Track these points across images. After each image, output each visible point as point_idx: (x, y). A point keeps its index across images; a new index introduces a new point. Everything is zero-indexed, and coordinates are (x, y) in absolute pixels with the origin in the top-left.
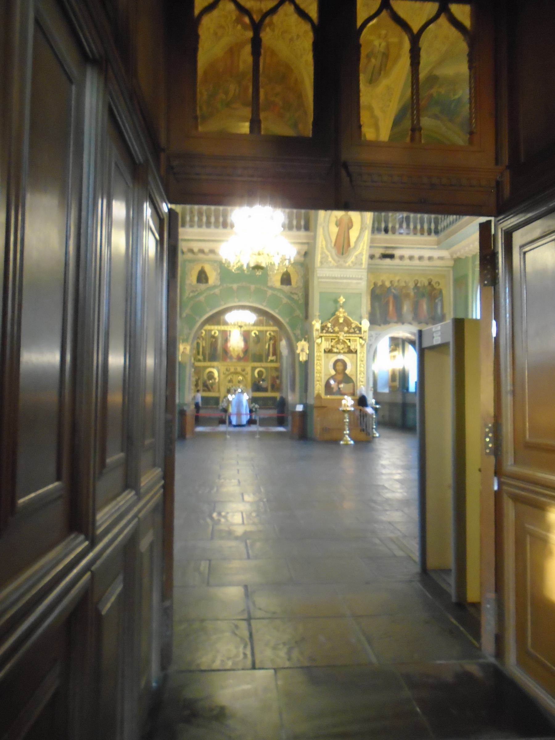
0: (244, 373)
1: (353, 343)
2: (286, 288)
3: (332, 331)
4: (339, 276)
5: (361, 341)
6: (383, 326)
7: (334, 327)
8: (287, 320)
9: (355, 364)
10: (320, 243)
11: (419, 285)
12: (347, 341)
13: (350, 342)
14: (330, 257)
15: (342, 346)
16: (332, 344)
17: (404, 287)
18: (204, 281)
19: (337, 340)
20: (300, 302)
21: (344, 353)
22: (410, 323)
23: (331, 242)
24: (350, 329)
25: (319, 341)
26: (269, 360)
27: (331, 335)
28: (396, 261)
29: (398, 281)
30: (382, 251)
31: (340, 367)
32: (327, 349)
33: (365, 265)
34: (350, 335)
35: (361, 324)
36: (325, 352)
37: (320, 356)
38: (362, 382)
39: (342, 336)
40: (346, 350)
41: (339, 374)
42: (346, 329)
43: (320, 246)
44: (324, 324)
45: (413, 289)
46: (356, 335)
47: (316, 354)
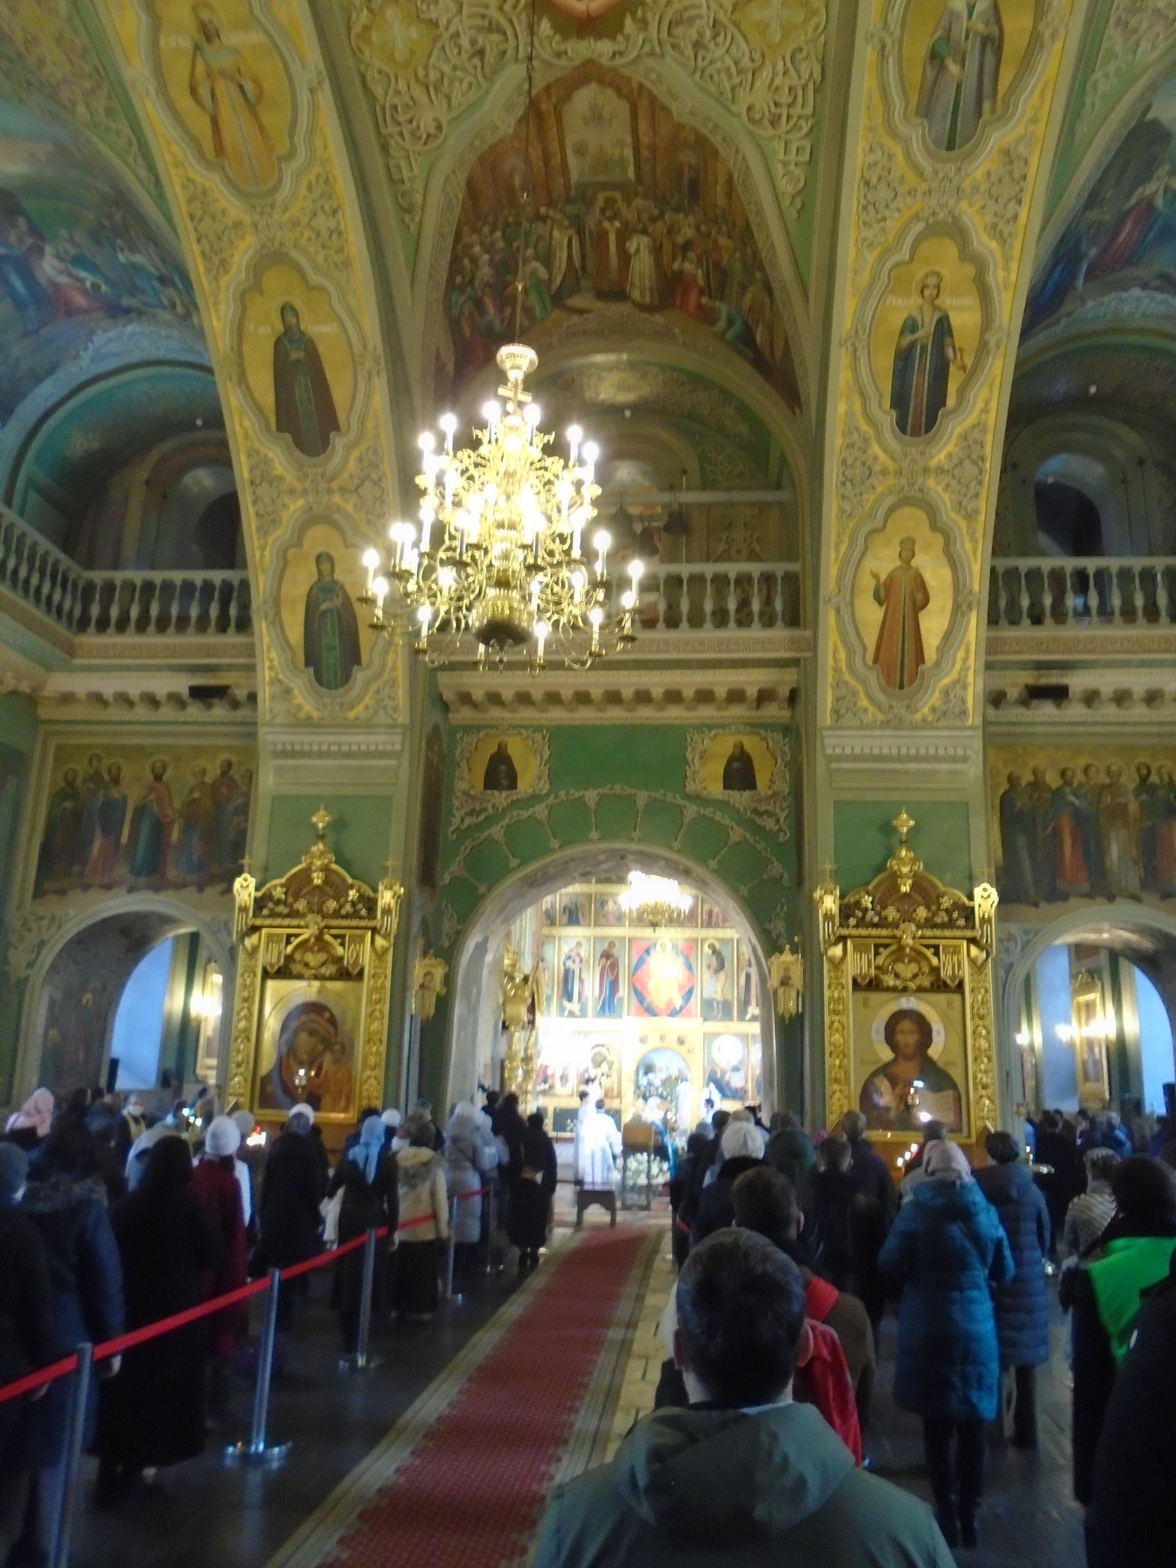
0: (683, 1049)
1: (949, 957)
2: (741, 798)
3: (876, 919)
4: (894, 751)
5: (974, 951)
6: (1044, 906)
7: (884, 907)
9: (959, 1029)
10: (830, 655)
11: (1154, 778)
12: (929, 953)
13: (937, 954)
14: (862, 695)
15: (914, 968)
16: (880, 960)
17: (1104, 788)
18: (505, 782)
19: (894, 947)
20: (782, 838)
21: (920, 990)
22: (1137, 899)
23: (865, 649)
24: (935, 914)
25: (837, 951)
26: (748, 1017)
27: (874, 932)
28: (1075, 711)
29: (1086, 770)
30: (1028, 678)
31: (908, 1036)
32: (864, 977)
33: (973, 718)
34: (938, 932)
35: (971, 897)
37: (840, 1000)
38: (985, 1087)
39: (909, 935)
40: (926, 982)
41: (908, 1058)
42: (922, 913)
43: (831, 663)
44: (851, 899)
45: (1137, 793)
46: (958, 933)
47: (827, 993)
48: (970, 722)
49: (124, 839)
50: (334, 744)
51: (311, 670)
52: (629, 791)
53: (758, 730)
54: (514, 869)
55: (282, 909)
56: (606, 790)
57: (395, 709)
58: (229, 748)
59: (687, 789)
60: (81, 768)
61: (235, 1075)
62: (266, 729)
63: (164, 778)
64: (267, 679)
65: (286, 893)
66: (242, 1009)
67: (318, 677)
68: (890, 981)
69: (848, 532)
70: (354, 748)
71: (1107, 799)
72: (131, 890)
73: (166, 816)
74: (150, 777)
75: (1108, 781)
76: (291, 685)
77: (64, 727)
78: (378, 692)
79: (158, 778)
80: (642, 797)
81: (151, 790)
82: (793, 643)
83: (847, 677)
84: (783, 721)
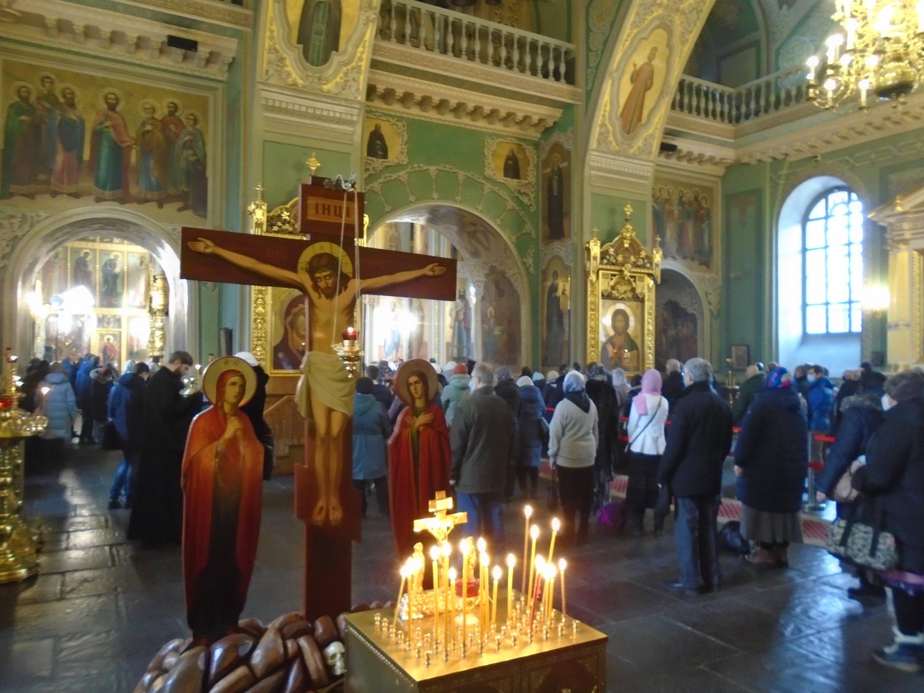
2: (512, 183)
3: (614, 261)
7: (617, 254)
8: (514, 238)
11: (684, 199)
12: (632, 280)
13: (635, 281)
14: (611, 134)
18: (380, 153)
20: (532, 209)
21: (629, 299)
22: (674, 258)
23: (618, 106)
24: (638, 261)
27: (613, 267)
29: (661, 189)
34: (638, 270)
36: (603, 295)
43: (602, 112)
48: (652, 159)
49: (86, 155)
50: (311, 107)
51: (301, 46)
52: (456, 171)
53: (521, 143)
54: (388, 212)
55: (287, 226)
56: (441, 168)
57: (358, 90)
58: (173, 93)
59: (485, 174)
60: (35, 88)
61: (257, 345)
62: (261, 86)
63: (119, 108)
64: (267, 46)
65: (289, 216)
66: (258, 298)
67: (306, 53)
68: (614, 292)
69: (632, 35)
70: (325, 113)
71: (667, 207)
72: (99, 200)
73: (124, 142)
74: (106, 107)
75: (667, 197)
76: (285, 55)
77: (12, 46)
78: (346, 74)
79: (112, 107)
80: (462, 174)
81: (107, 117)
82: (573, 95)
83: (607, 122)
84: (535, 139)
